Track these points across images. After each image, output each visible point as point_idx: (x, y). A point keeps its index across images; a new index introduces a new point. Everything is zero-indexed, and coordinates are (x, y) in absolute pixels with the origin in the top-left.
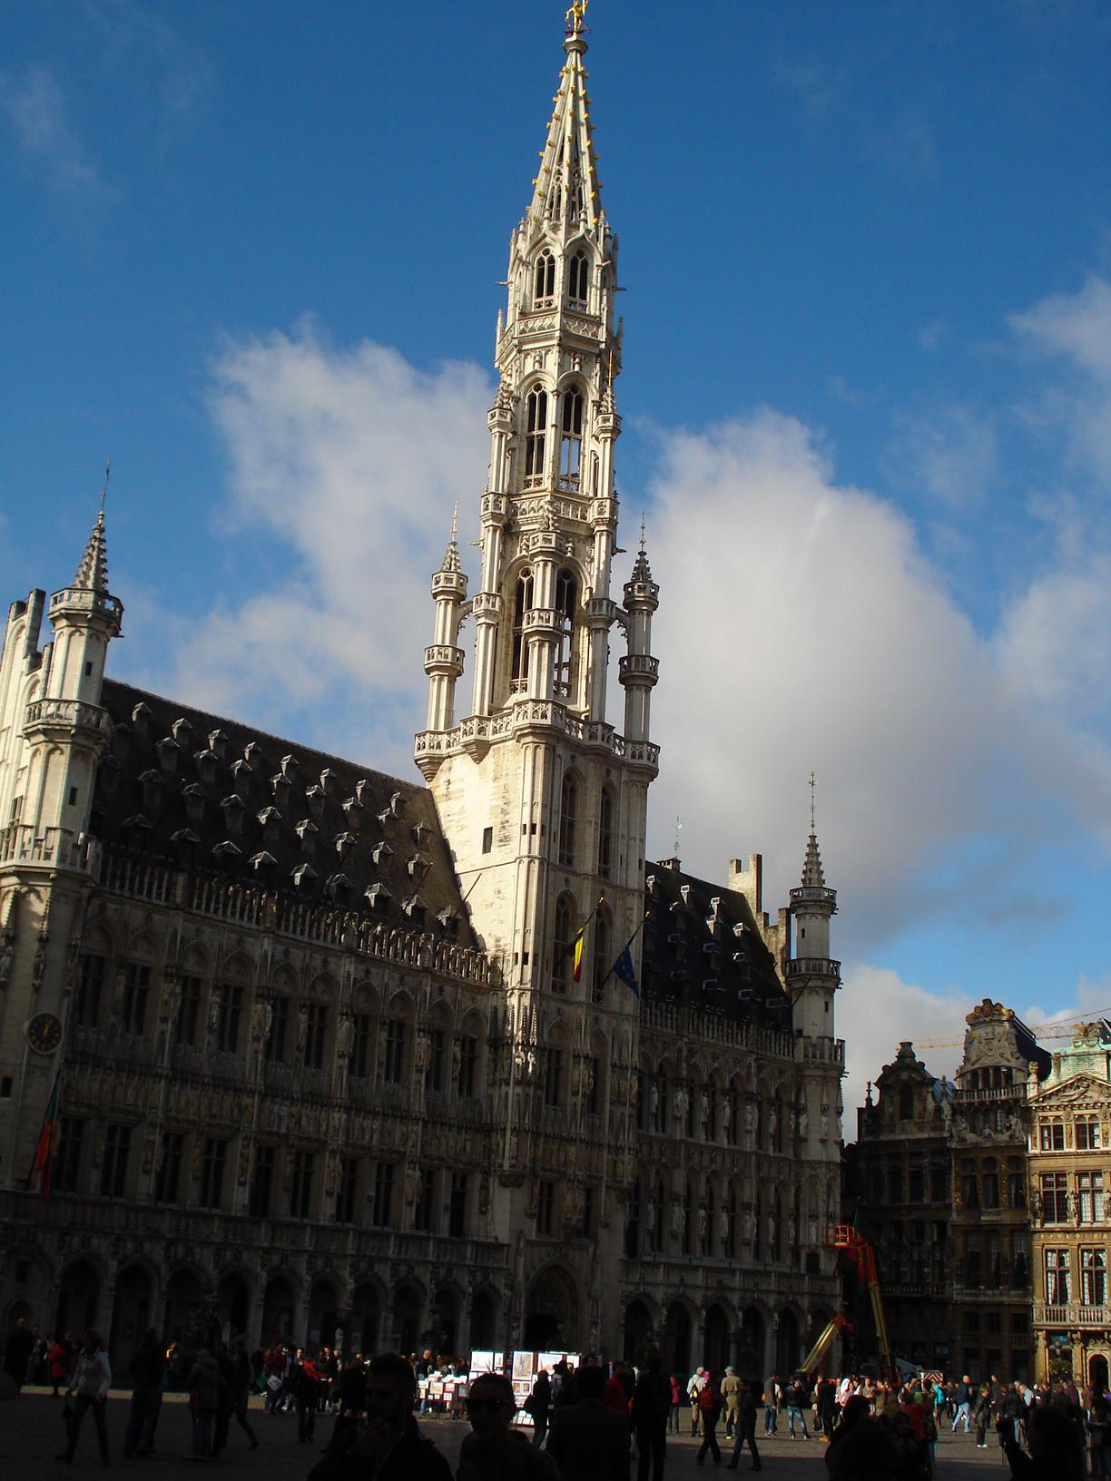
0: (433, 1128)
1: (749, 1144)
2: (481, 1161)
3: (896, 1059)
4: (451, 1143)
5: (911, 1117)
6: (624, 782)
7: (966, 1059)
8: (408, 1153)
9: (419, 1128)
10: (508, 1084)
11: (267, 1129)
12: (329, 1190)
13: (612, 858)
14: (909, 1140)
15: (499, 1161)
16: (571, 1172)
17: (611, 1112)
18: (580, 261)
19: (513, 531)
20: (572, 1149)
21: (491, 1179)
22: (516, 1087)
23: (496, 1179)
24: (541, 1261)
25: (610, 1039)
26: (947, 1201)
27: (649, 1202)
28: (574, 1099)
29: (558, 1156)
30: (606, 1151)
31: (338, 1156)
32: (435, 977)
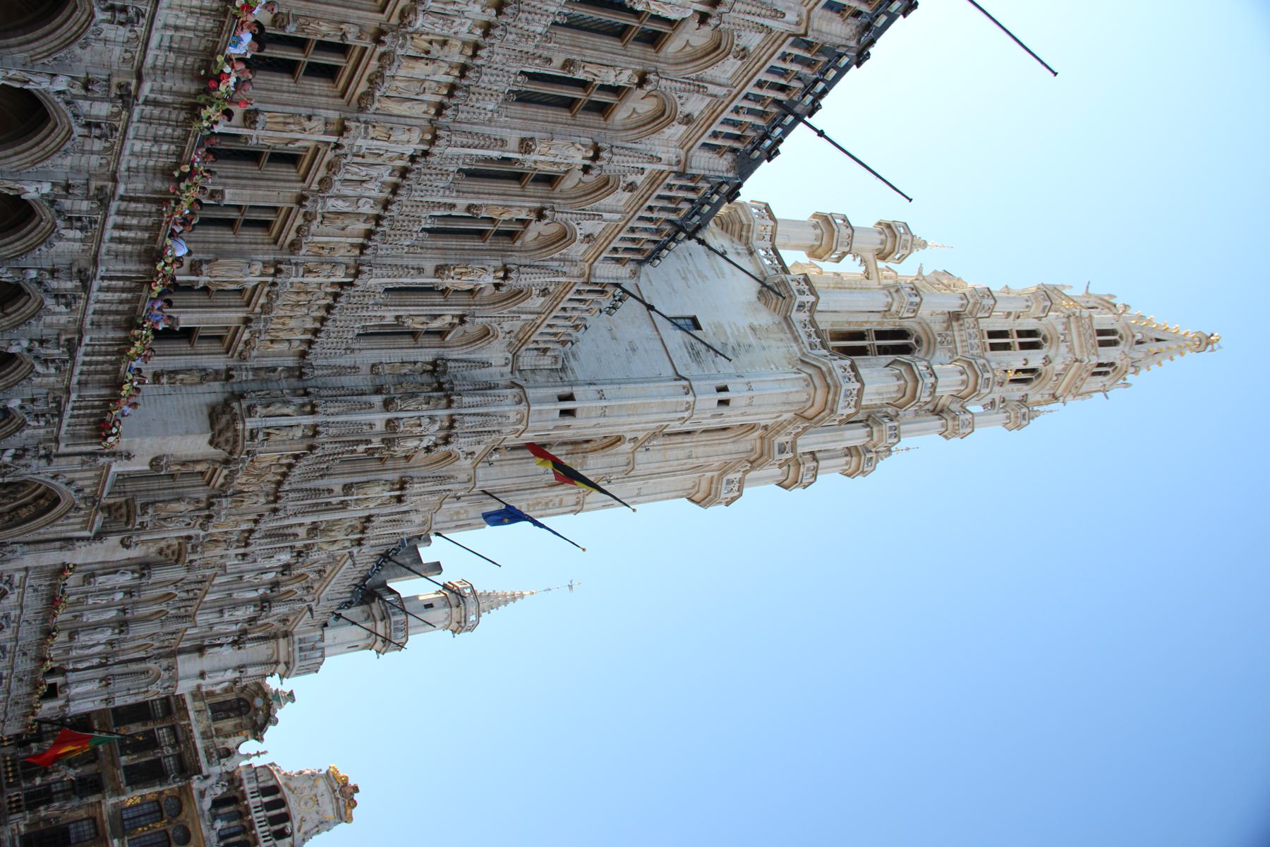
2: (248, 364)
3: (274, 689)
4: (292, 323)
5: (215, 719)
7: (288, 777)
8: (294, 259)
9: (340, 276)
10: (387, 405)
12: (261, 118)
14: (190, 725)
15: (259, 409)
16: (224, 505)
17: (301, 525)
19: (954, 324)
20: (263, 500)
21: (216, 386)
23: (220, 398)
24: (69, 483)
26: (128, 788)
28: (338, 489)
31: (333, 139)
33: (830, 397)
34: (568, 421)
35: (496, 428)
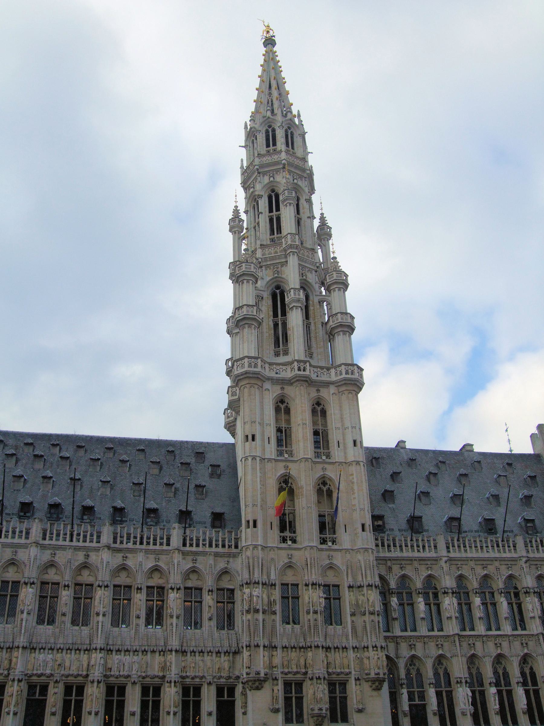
0: (191, 655)
1: (535, 628)
4: (209, 664)
6: (333, 394)
9: (172, 658)
11: (35, 672)
13: (330, 445)
17: (353, 622)
18: (270, 130)
20: (310, 654)
22: (247, 615)
25: (343, 568)
27: (430, 687)
29: (299, 661)
30: (352, 651)
31: (96, 684)
32: (184, 554)
33: (241, 377)
34: (251, 524)
35: (251, 560)
